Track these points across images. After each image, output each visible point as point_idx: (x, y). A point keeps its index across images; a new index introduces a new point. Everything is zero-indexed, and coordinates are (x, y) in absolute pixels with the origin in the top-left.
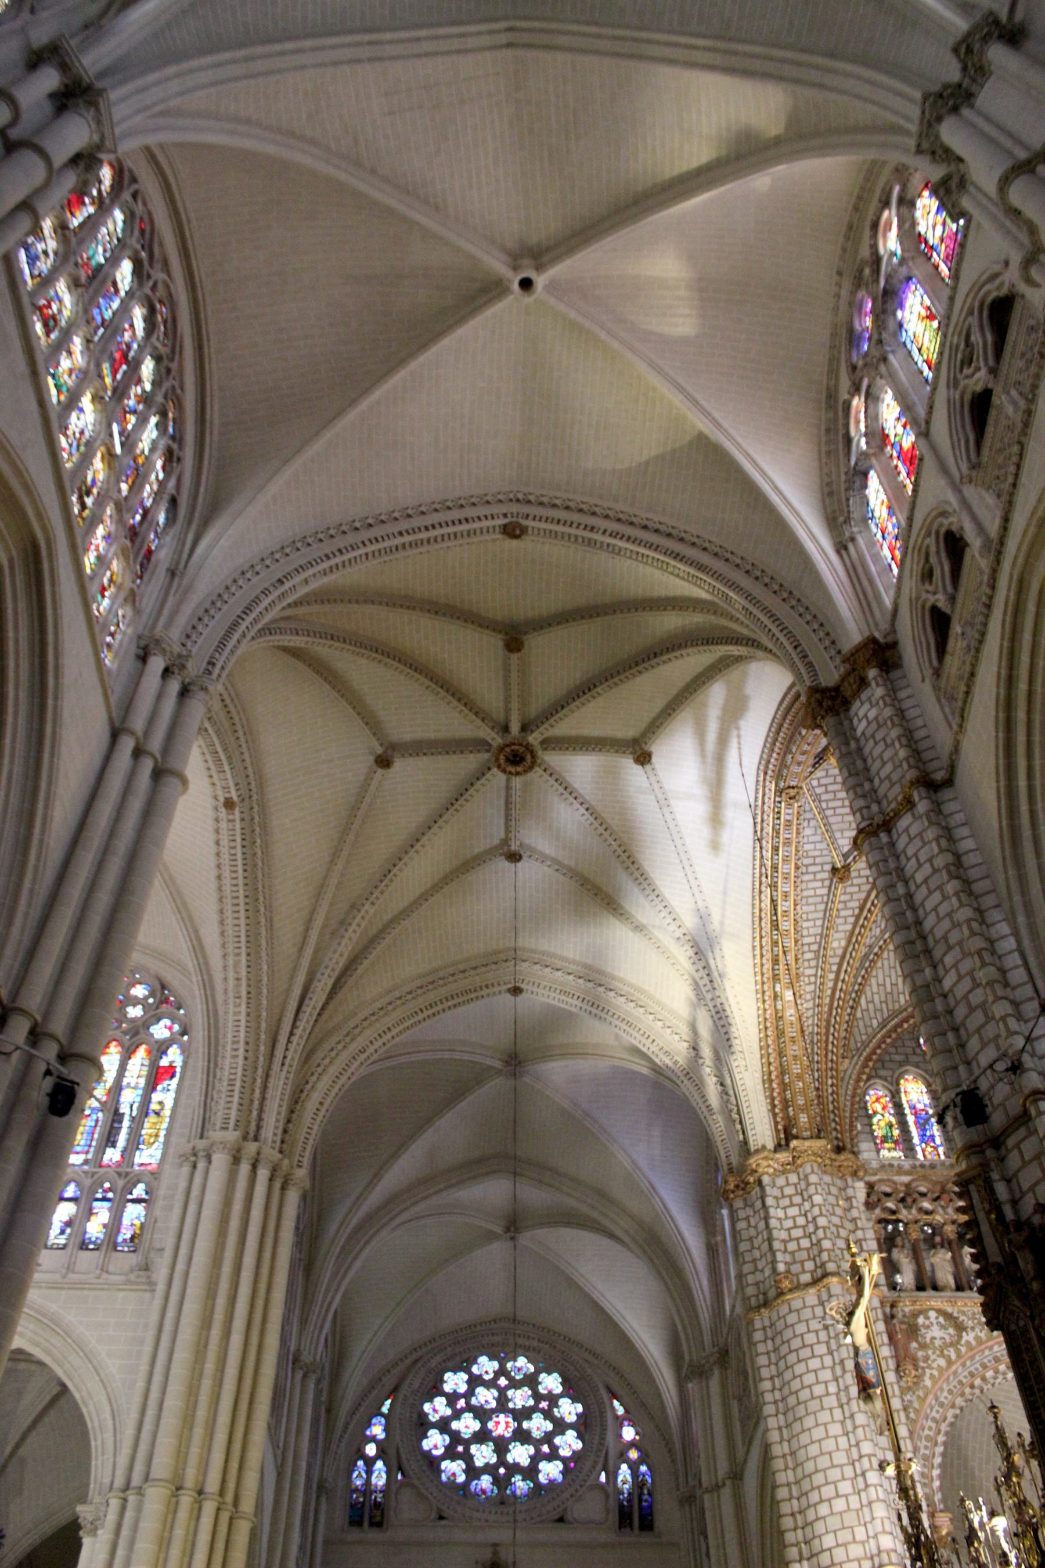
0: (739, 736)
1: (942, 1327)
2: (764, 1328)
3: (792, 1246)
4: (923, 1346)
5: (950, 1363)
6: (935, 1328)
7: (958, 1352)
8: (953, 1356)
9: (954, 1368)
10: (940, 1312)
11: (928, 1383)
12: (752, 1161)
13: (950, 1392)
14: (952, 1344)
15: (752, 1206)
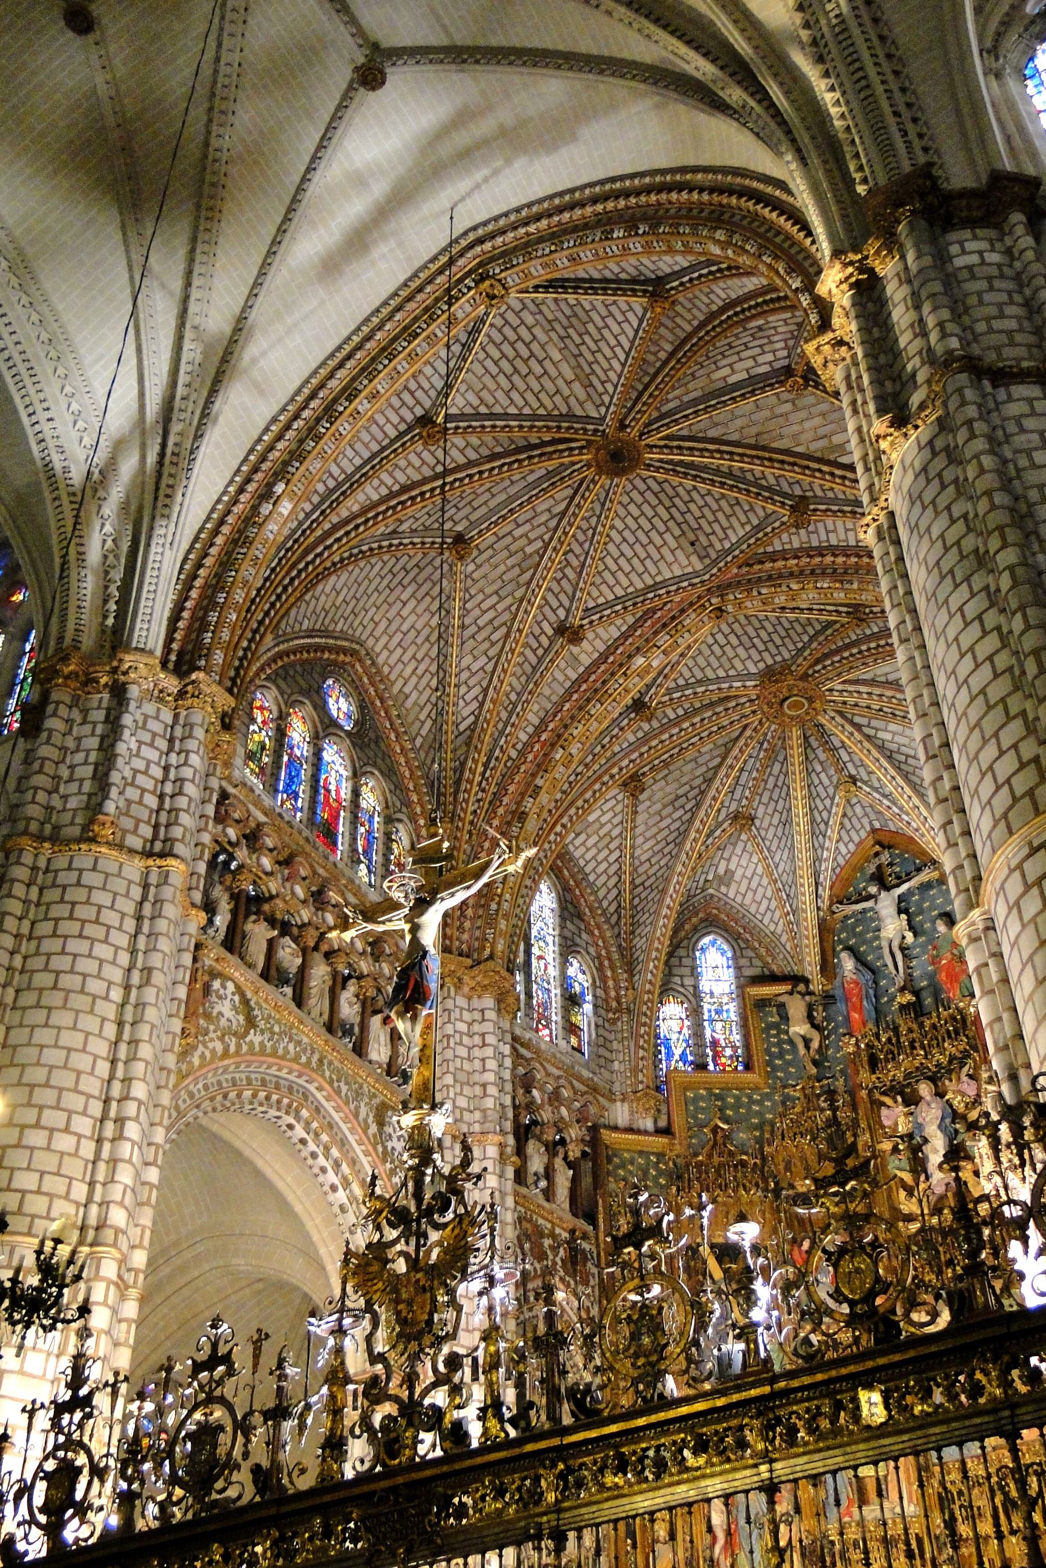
0: (496, 172)
1: (234, 1008)
2: (34, 868)
3: (132, 793)
4: (207, 1016)
5: (226, 1054)
6: (227, 1003)
7: (239, 1046)
8: (232, 1049)
9: (226, 1062)
10: (239, 990)
11: (196, 1061)
12: (127, 657)
13: (206, 1087)
14: (235, 1034)
15: (85, 712)
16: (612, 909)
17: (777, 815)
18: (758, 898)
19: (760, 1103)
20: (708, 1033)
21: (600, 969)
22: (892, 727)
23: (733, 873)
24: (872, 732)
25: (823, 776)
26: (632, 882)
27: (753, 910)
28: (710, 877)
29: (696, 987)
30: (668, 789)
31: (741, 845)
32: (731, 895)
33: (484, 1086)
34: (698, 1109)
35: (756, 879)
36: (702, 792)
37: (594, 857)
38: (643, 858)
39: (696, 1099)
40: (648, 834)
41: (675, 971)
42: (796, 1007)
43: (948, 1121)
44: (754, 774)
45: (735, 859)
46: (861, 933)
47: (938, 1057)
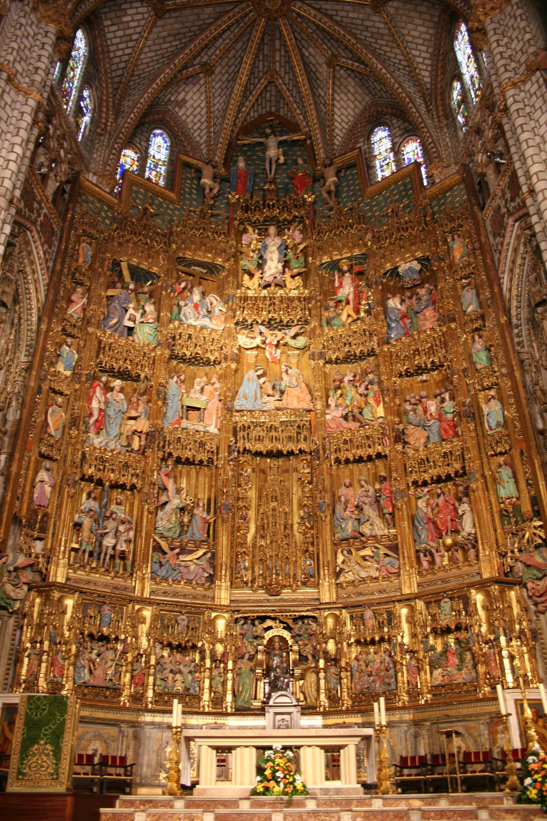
16: (117, 80)
17: (227, 75)
18: (196, 120)
19: (173, 210)
20: (147, 174)
21: (100, 105)
22: (311, 50)
23: (186, 102)
24: (301, 46)
25: (261, 63)
26: (133, 71)
27: (190, 126)
28: (172, 99)
29: (147, 149)
30: (176, 26)
31: (198, 86)
32: (180, 114)
33: (37, 69)
34: (137, 197)
35: (199, 109)
36: (195, 35)
37: (117, 44)
38: (145, 61)
39: (137, 192)
40: (153, 48)
41: (138, 135)
42: (208, 171)
43: (283, 247)
44: (218, 52)
45: (191, 94)
46: (250, 156)
47: (286, 215)
